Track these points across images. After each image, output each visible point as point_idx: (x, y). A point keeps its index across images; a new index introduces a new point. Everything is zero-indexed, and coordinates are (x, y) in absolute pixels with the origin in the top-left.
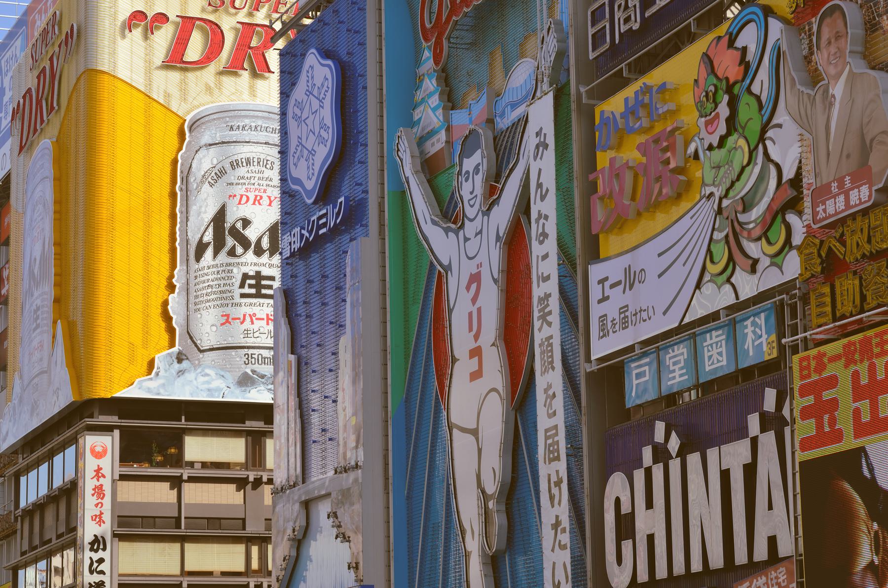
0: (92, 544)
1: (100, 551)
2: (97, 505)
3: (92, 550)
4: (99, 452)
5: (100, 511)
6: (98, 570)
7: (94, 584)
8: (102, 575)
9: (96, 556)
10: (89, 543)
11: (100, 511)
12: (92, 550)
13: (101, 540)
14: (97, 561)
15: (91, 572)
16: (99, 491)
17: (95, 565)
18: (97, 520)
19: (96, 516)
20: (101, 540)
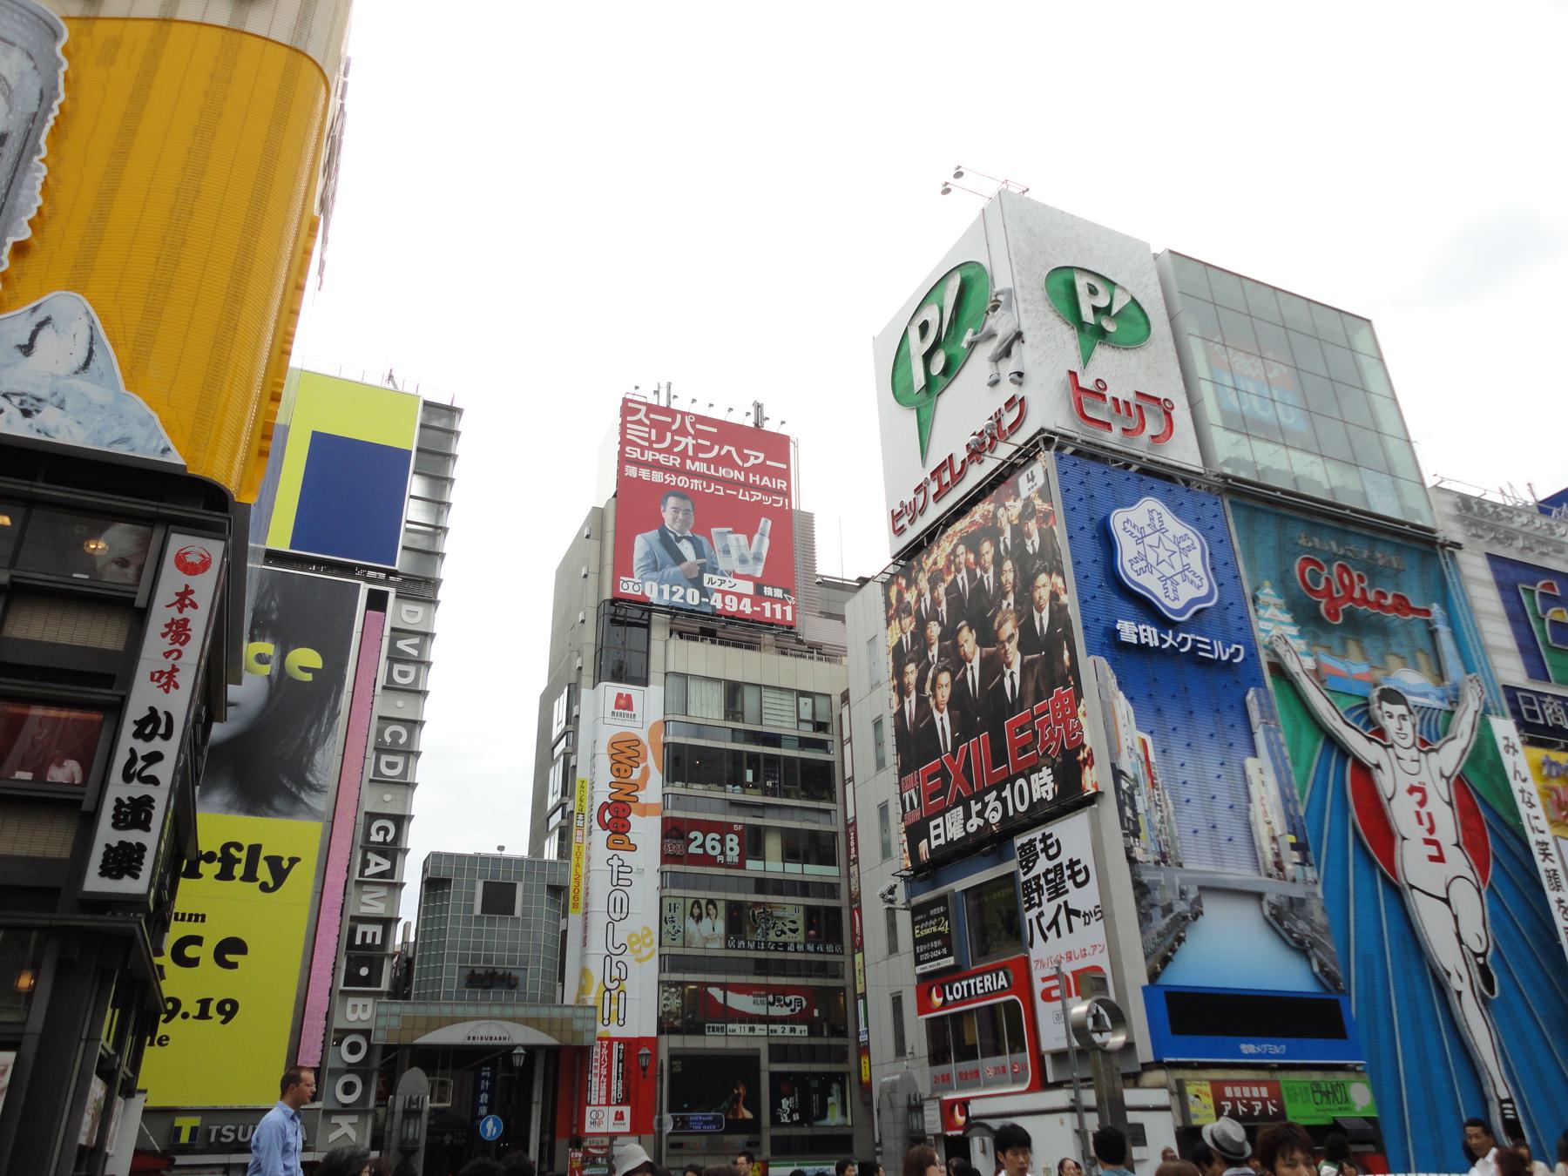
0: (141, 724)
1: (157, 739)
2: (167, 654)
3: (137, 735)
4: (192, 564)
5: (173, 666)
6: (144, 774)
7: (127, 802)
8: (151, 786)
9: (143, 748)
10: (135, 722)
11: (173, 666)
12: (138, 734)
13: (163, 719)
14: (143, 758)
15: (127, 777)
16: (179, 631)
17: (140, 764)
18: (164, 680)
19: (162, 673)
20: (163, 719)
